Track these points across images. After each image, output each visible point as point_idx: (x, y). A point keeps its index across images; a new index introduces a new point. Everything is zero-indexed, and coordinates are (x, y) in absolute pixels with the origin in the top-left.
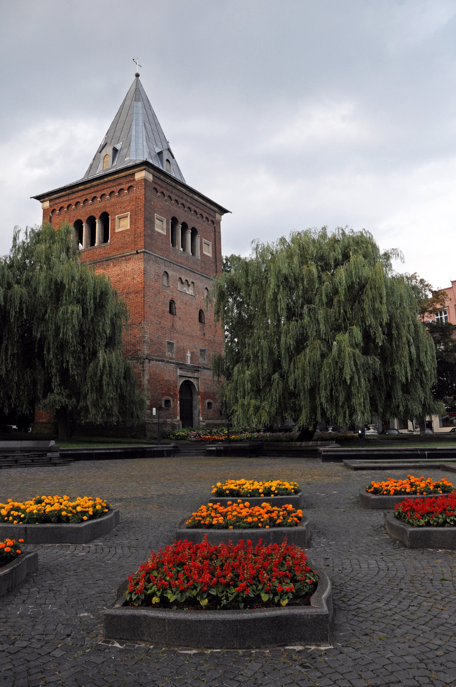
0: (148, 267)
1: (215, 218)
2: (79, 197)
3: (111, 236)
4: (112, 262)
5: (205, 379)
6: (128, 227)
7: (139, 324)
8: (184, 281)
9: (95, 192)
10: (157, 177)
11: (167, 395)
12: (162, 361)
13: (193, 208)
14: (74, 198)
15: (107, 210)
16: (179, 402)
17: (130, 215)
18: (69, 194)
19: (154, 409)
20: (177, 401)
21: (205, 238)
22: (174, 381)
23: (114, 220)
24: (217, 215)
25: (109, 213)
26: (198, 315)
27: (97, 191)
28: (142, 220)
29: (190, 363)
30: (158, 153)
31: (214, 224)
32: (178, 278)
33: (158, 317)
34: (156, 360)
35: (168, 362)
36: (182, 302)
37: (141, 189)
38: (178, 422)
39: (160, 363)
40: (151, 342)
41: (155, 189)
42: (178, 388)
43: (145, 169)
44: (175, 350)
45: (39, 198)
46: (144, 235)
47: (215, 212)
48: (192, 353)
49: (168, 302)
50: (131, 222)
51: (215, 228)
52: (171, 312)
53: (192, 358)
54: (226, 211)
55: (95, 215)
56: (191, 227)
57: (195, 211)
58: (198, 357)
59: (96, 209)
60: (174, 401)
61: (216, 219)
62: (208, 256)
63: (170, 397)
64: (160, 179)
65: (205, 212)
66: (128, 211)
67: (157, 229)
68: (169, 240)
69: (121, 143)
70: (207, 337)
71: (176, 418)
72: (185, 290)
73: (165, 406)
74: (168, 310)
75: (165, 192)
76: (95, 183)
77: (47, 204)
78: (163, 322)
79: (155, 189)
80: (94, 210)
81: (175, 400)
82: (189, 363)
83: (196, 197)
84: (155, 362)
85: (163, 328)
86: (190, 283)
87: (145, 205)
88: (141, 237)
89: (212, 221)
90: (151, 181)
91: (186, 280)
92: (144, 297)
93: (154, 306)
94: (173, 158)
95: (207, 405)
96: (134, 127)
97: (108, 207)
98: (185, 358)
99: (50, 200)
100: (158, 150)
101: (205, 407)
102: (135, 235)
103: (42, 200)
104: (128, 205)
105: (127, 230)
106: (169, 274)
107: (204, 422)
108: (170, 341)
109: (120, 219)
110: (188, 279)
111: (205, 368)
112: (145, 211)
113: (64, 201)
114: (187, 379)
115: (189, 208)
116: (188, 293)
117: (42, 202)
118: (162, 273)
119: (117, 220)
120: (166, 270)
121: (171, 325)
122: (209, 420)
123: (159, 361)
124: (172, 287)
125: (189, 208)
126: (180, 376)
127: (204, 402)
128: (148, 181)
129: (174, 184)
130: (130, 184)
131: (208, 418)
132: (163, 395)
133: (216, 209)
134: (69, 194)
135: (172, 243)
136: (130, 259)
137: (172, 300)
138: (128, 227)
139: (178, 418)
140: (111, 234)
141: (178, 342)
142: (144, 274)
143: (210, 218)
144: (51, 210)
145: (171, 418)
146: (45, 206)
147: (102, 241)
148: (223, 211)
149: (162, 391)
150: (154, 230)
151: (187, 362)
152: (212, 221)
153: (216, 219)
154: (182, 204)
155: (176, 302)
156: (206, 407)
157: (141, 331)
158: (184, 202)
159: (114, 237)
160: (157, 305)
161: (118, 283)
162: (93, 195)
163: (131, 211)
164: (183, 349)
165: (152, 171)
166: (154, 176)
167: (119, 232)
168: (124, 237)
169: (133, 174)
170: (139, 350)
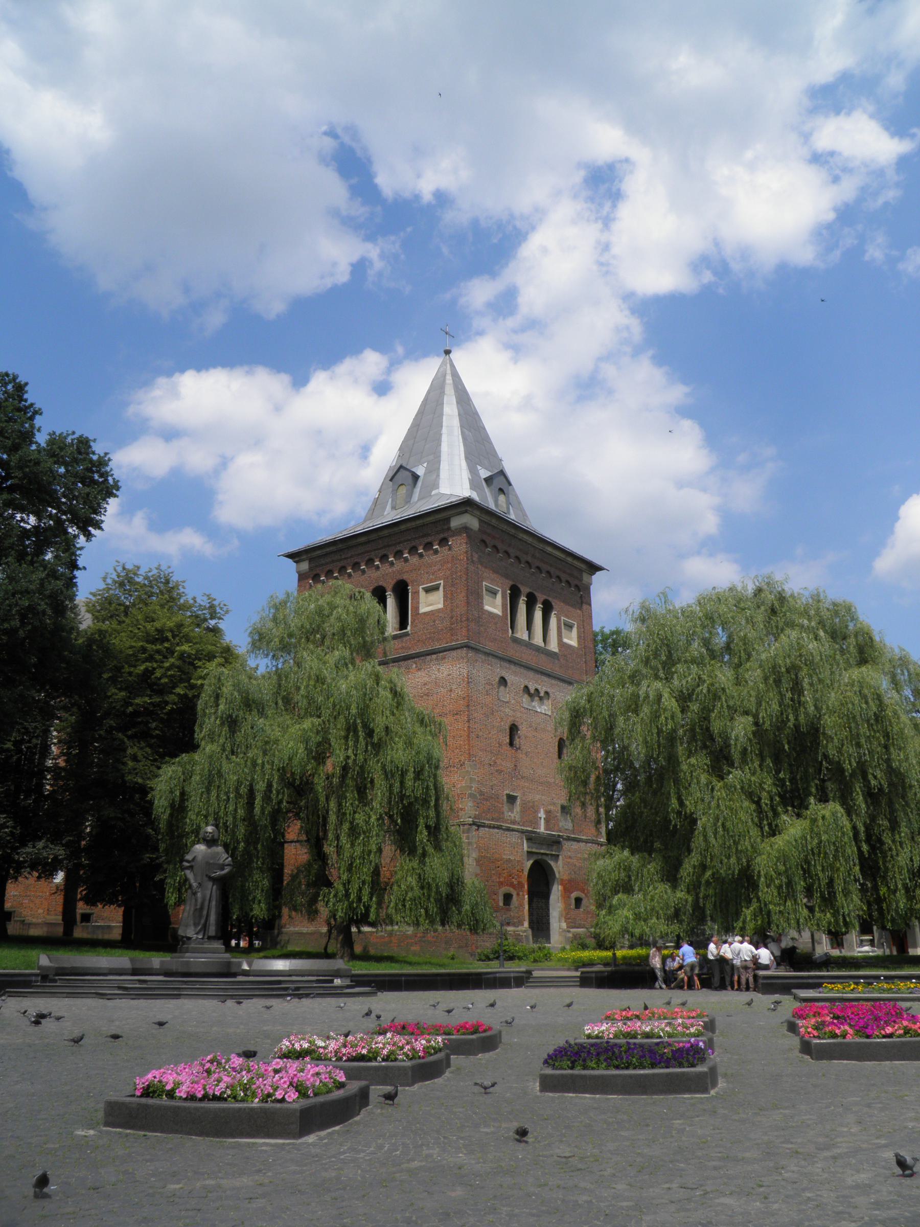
0: (474, 672)
1: (581, 580)
2: (359, 554)
3: (412, 618)
4: (416, 664)
5: (570, 857)
6: (441, 606)
7: (461, 765)
8: (532, 691)
9: (385, 547)
10: (486, 522)
11: (507, 885)
12: (499, 827)
13: (544, 567)
14: (351, 557)
15: (405, 577)
16: (526, 897)
17: (444, 586)
18: (341, 550)
20: (524, 895)
21: (566, 616)
22: (518, 861)
23: (416, 593)
24: (585, 577)
25: (408, 581)
26: (557, 748)
27: (389, 546)
28: (464, 594)
29: (546, 829)
30: (485, 479)
31: (579, 590)
32: (522, 686)
33: (492, 753)
34: (490, 827)
35: (508, 829)
36: (530, 727)
37: (460, 544)
38: (525, 931)
39: (496, 830)
40: (480, 795)
41: (483, 541)
42: (526, 873)
43: (466, 512)
45: (292, 556)
46: (468, 619)
47: (581, 571)
48: (548, 812)
49: (507, 728)
50: (445, 596)
51: (581, 597)
52: (511, 744)
53: (547, 821)
54: (599, 568)
55: (384, 585)
56: (542, 600)
57: (548, 572)
58: (558, 820)
59: (387, 574)
60: (518, 894)
61: (584, 582)
62: (570, 646)
63: (511, 889)
64: (490, 525)
65: (564, 572)
66: (440, 580)
67: (487, 608)
68: (507, 624)
69: (425, 465)
71: (523, 925)
72: (534, 707)
73: (504, 904)
74: (508, 741)
75: (500, 546)
76: (386, 532)
77: (305, 566)
78: (499, 762)
79: (483, 541)
80: (383, 575)
81: (521, 893)
82: (542, 829)
83: (549, 549)
85: (500, 772)
86: (542, 694)
87: (467, 569)
88: (461, 621)
89: (577, 586)
90: (477, 530)
91: (537, 690)
92: (468, 721)
93: (486, 736)
94: (510, 484)
95: (573, 902)
96: (444, 438)
97: (407, 572)
98: (535, 822)
99: (311, 560)
100: (484, 473)
101: (570, 905)
102: (452, 618)
103: (296, 559)
104: (439, 570)
105: (439, 611)
106: (508, 681)
107: (569, 932)
108: (511, 793)
109: (428, 590)
110: (539, 687)
111: (569, 839)
112: (467, 579)
113: (333, 561)
114: (540, 857)
115: (538, 568)
116: (539, 710)
117: (296, 562)
118: (497, 679)
119: (422, 594)
120: (503, 675)
122: (578, 928)
123: (494, 827)
124: (513, 702)
125: (538, 568)
127: (569, 897)
128: (472, 530)
129: (513, 531)
130: (442, 536)
132: (501, 884)
133: (583, 566)
134: (341, 550)
135: (511, 628)
136: (445, 658)
137: (513, 725)
138: (441, 606)
139: (526, 924)
140: (412, 616)
141: (524, 794)
142: (468, 683)
143: (574, 582)
144: (312, 576)
145: (514, 925)
146: (301, 569)
147: (397, 626)
148: (594, 568)
149: (499, 878)
150: (482, 609)
151: (540, 828)
152: (577, 586)
153: (584, 582)
154: (527, 562)
155: (520, 727)
156: (573, 906)
157: (464, 778)
158: (529, 559)
159: (417, 621)
160: (490, 733)
161: (425, 697)
162: (382, 552)
163: (446, 579)
164: (533, 807)
165: (478, 513)
166: (480, 520)
167: (425, 613)
168: (434, 621)
169: (448, 520)
170: (462, 809)
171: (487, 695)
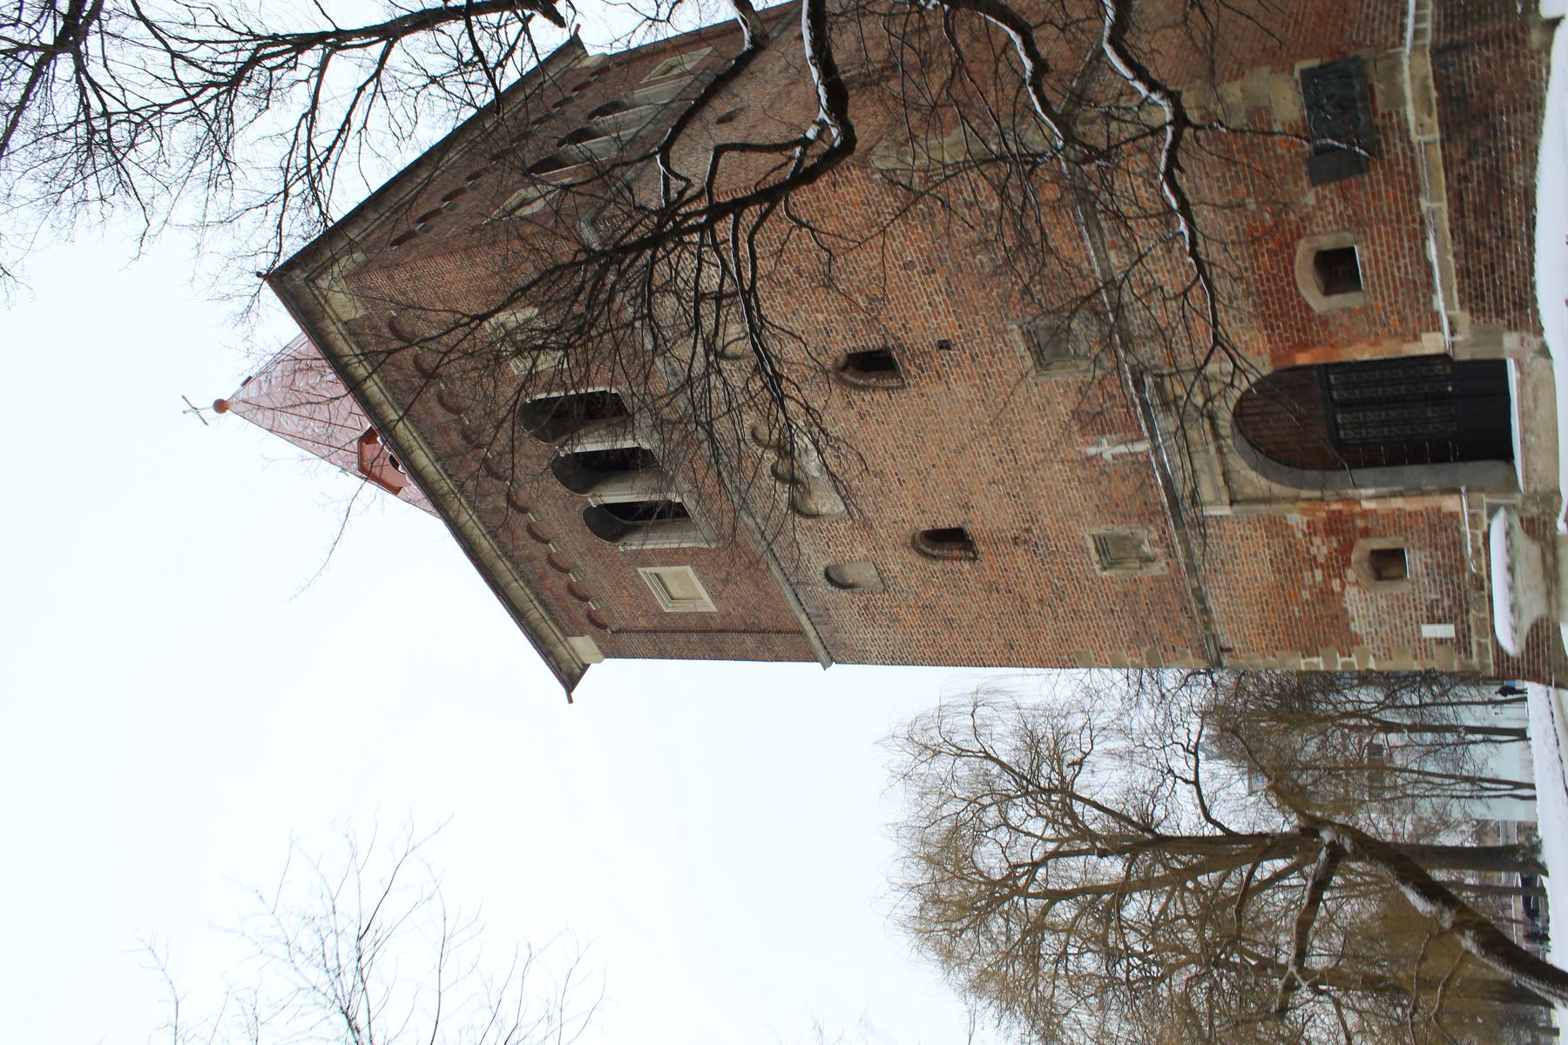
10: (555, 621)
19: (1430, 631)
20: (1365, 514)
34: (1207, 625)
39: (1211, 603)
44: (1120, 530)
60: (1366, 533)
70: (946, 326)
71: (1454, 516)
81: (1360, 523)
84: (1218, 629)
95: (1337, 301)
121: (1020, 551)
123: (1206, 611)
126: (1232, 502)
127: (1324, 322)
128: (600, 647)
131: (1420, 278)
139: (1450, 504)
165: (561, 648)
171: (898, 620)
